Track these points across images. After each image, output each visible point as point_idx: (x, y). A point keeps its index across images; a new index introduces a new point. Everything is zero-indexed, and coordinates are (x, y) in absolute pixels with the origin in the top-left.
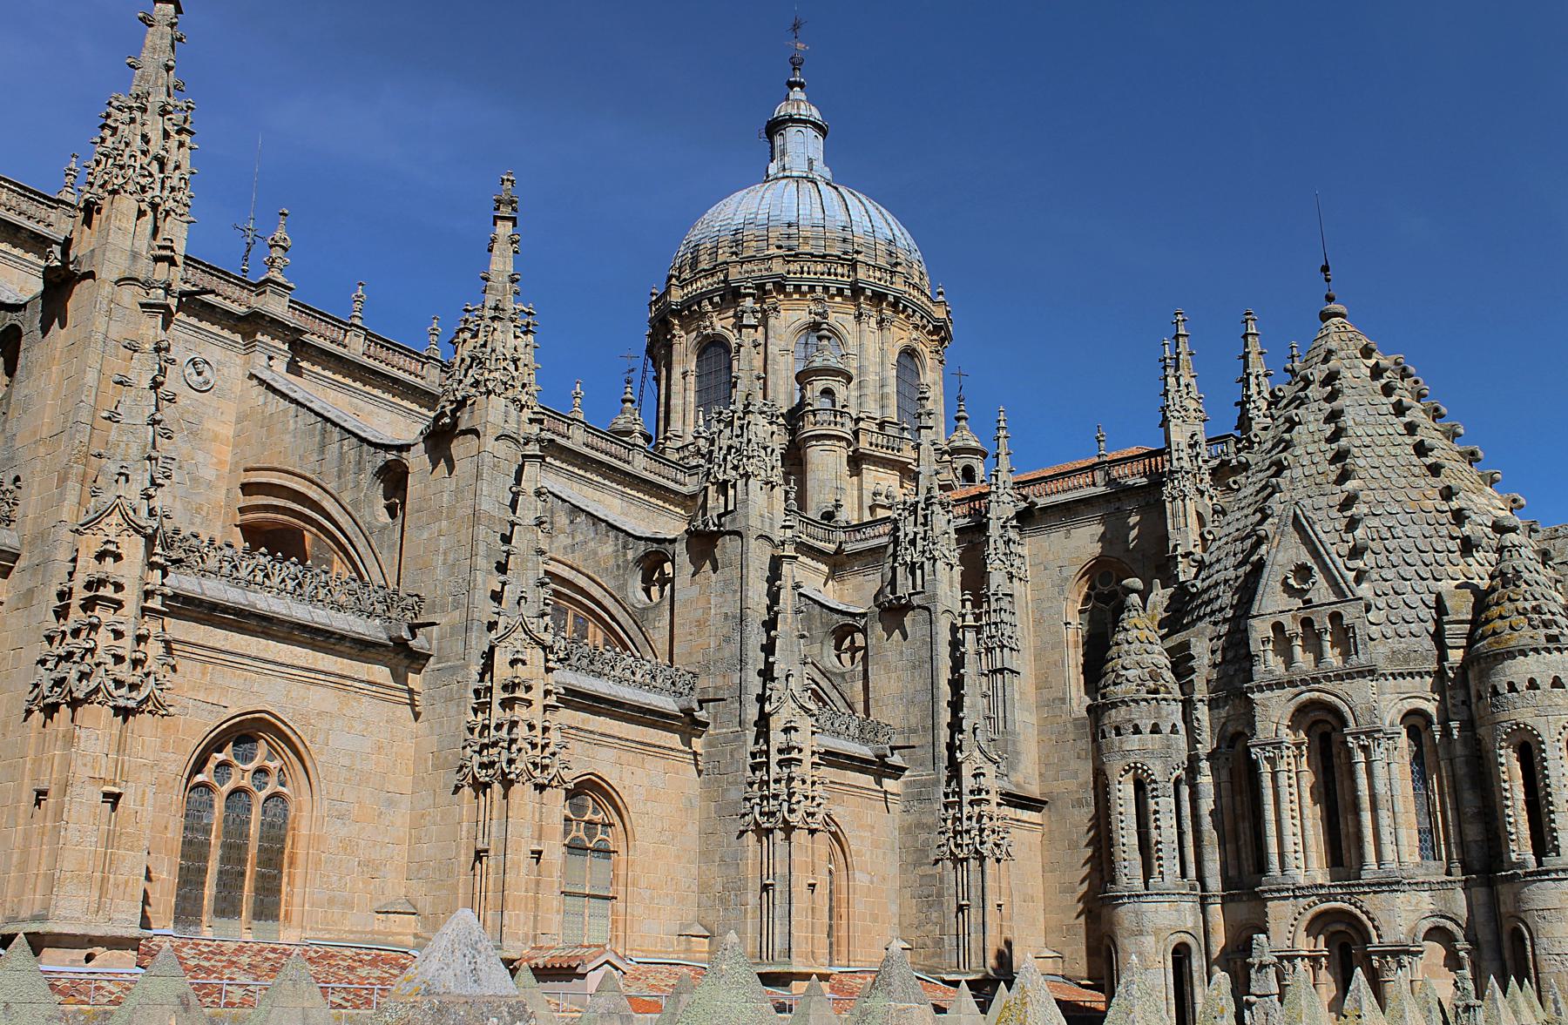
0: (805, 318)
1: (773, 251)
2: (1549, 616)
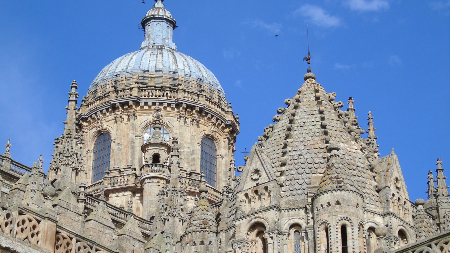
0: (150, 118)
2: (341, 179)
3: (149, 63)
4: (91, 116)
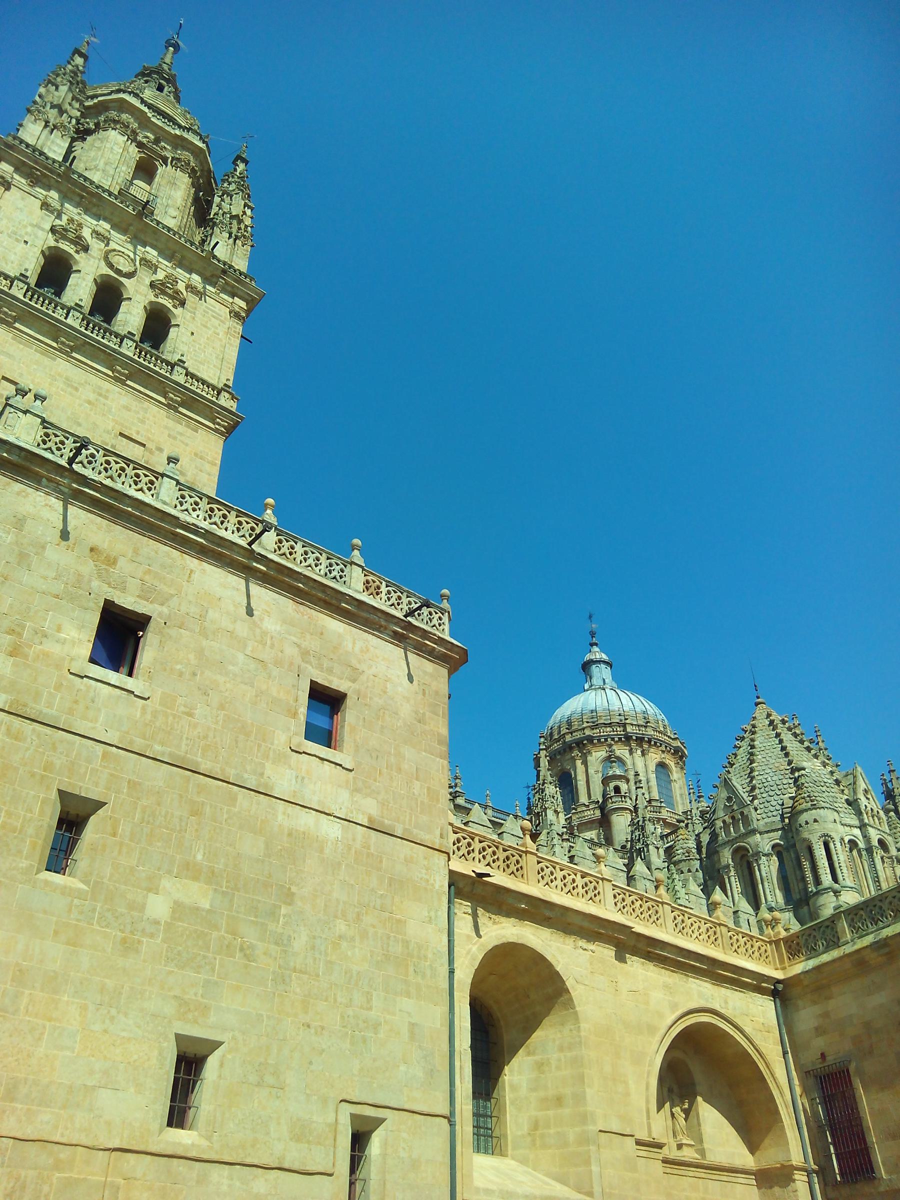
1: (585, 725)
2: (814, 798)
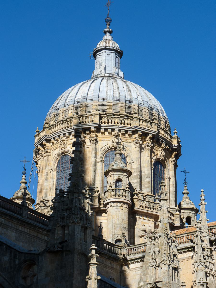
3: (107, 92)
4: (54, 138)
